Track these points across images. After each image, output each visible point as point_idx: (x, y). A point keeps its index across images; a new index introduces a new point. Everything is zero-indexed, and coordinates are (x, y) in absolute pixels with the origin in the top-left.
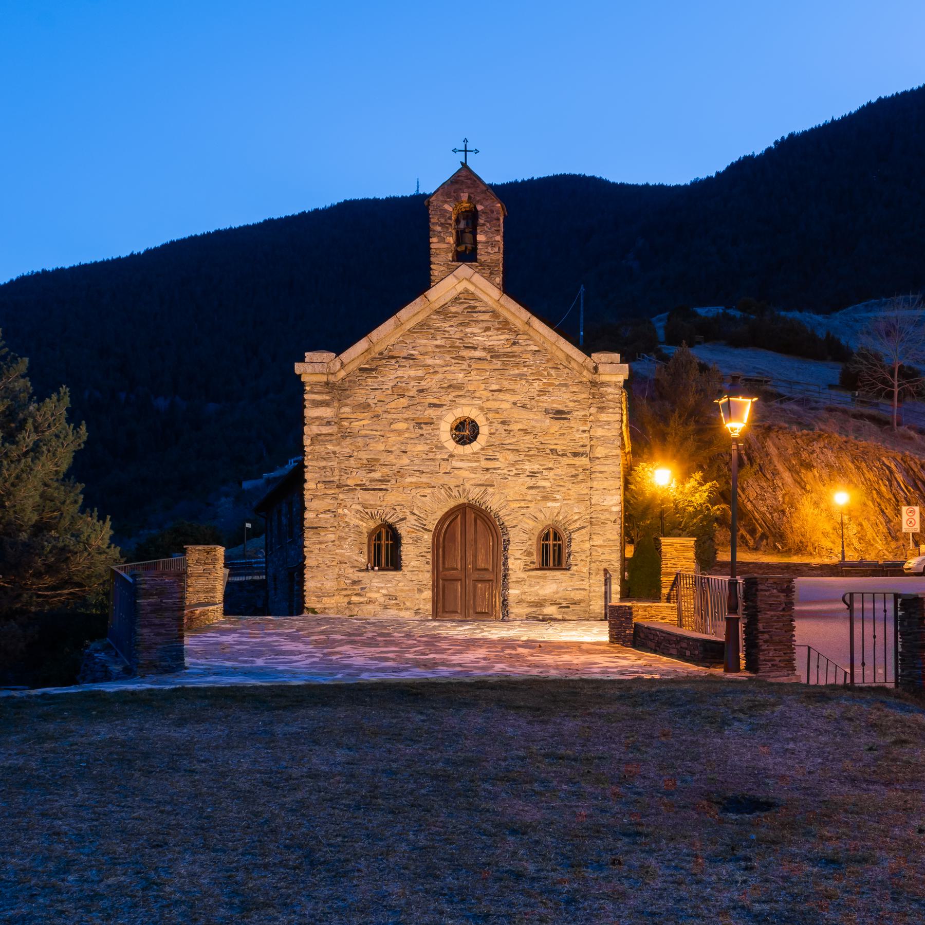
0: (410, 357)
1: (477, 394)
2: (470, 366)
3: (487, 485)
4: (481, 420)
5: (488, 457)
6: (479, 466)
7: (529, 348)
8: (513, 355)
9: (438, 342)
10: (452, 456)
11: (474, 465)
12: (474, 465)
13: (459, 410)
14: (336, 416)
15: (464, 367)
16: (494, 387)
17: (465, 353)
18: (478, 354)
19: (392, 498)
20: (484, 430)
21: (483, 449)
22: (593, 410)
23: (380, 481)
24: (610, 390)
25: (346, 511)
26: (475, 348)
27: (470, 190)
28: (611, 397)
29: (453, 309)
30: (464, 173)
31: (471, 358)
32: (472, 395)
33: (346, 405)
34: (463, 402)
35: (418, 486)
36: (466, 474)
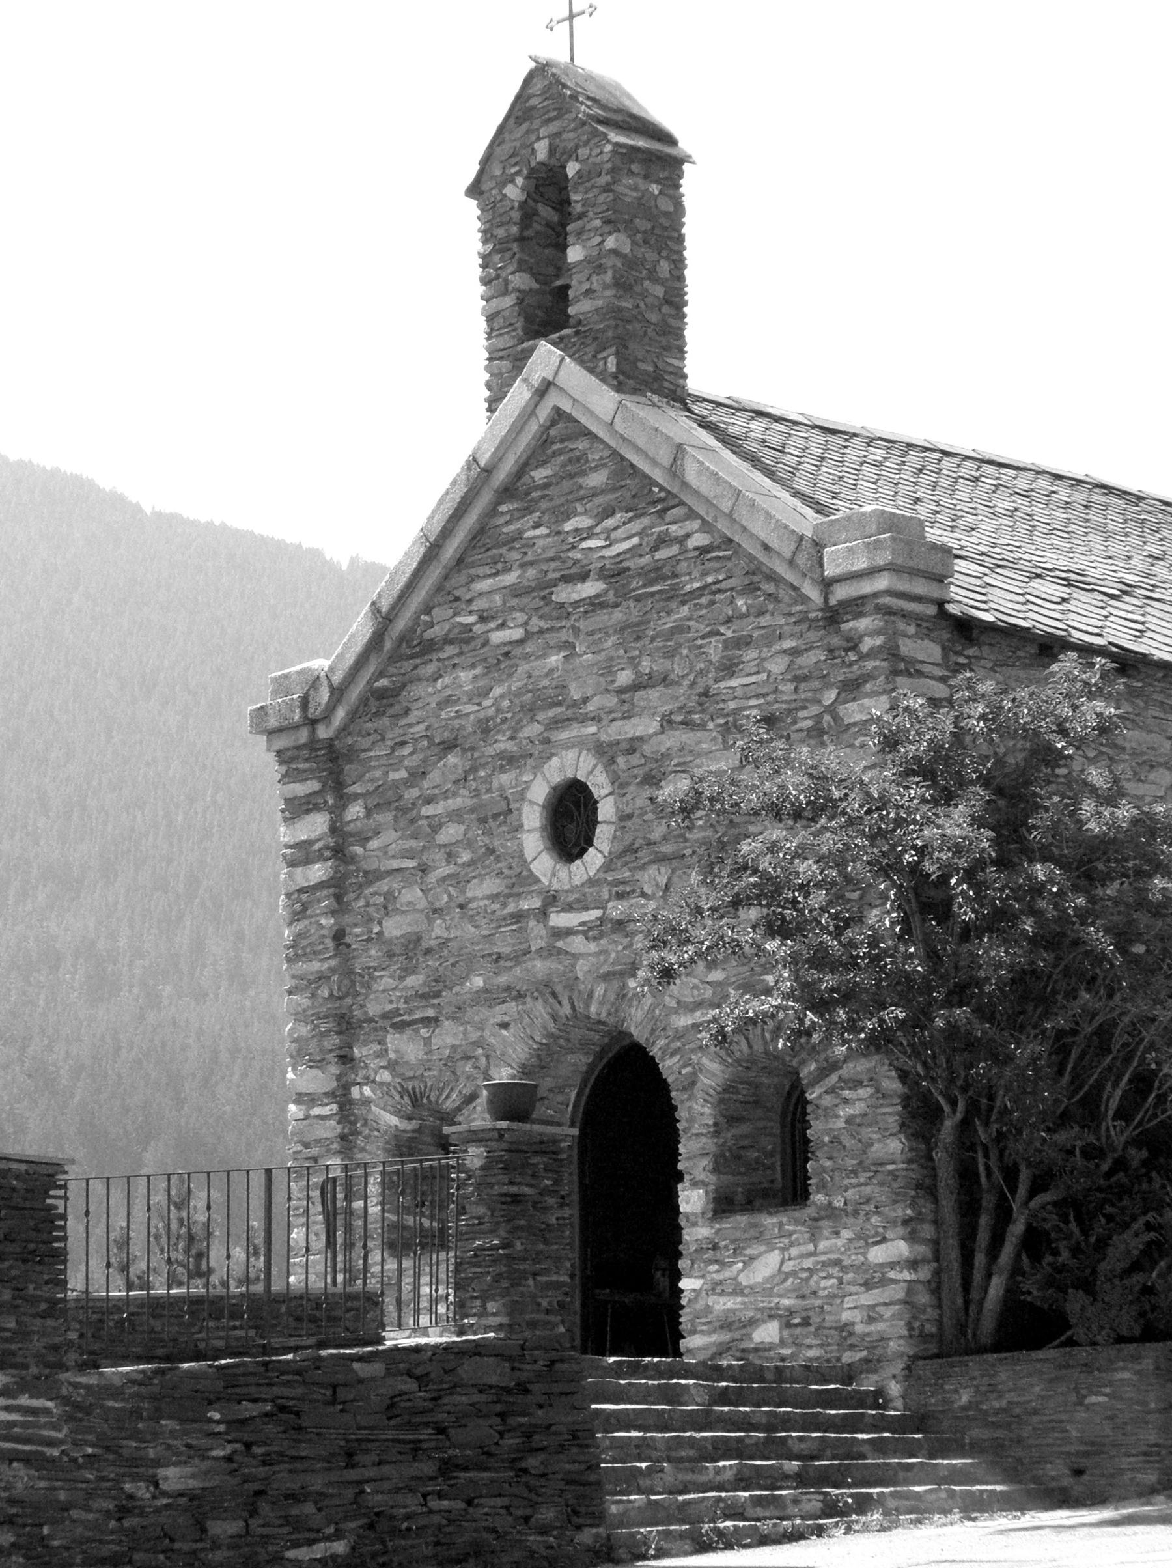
0: (463, 638)
1: (590, 707)
2: (576, 631)
3: (622, 974)
4: (599, 784)
5: (621, 888)
6: (602, 920)
7: (693, 542)
8: (656, 573)
9: (510, 578)
10: (551, 900)
11: (593, 915)
12: (593, 915)
13: (555, 761)
14: (333, 830)
15: (564, 636)
16: (624, 677)
17: (565, 594)
18: (590, 588)
19: (448, 1036)
20: (606, 810)
21: (607, 867)
22: (830, 696)
23: (424, 996)
24: (863, 624)
25: (367, 1091)
26: (584, 577)
27: (553, 127)
28: (867, 644)
29: (540, 475)
30: (539, 85)
31: (576, 604)
32: (576, 713)
33: (356, 797)
34: (563, 735)
35: (487, 997)
36: (578, 944)
